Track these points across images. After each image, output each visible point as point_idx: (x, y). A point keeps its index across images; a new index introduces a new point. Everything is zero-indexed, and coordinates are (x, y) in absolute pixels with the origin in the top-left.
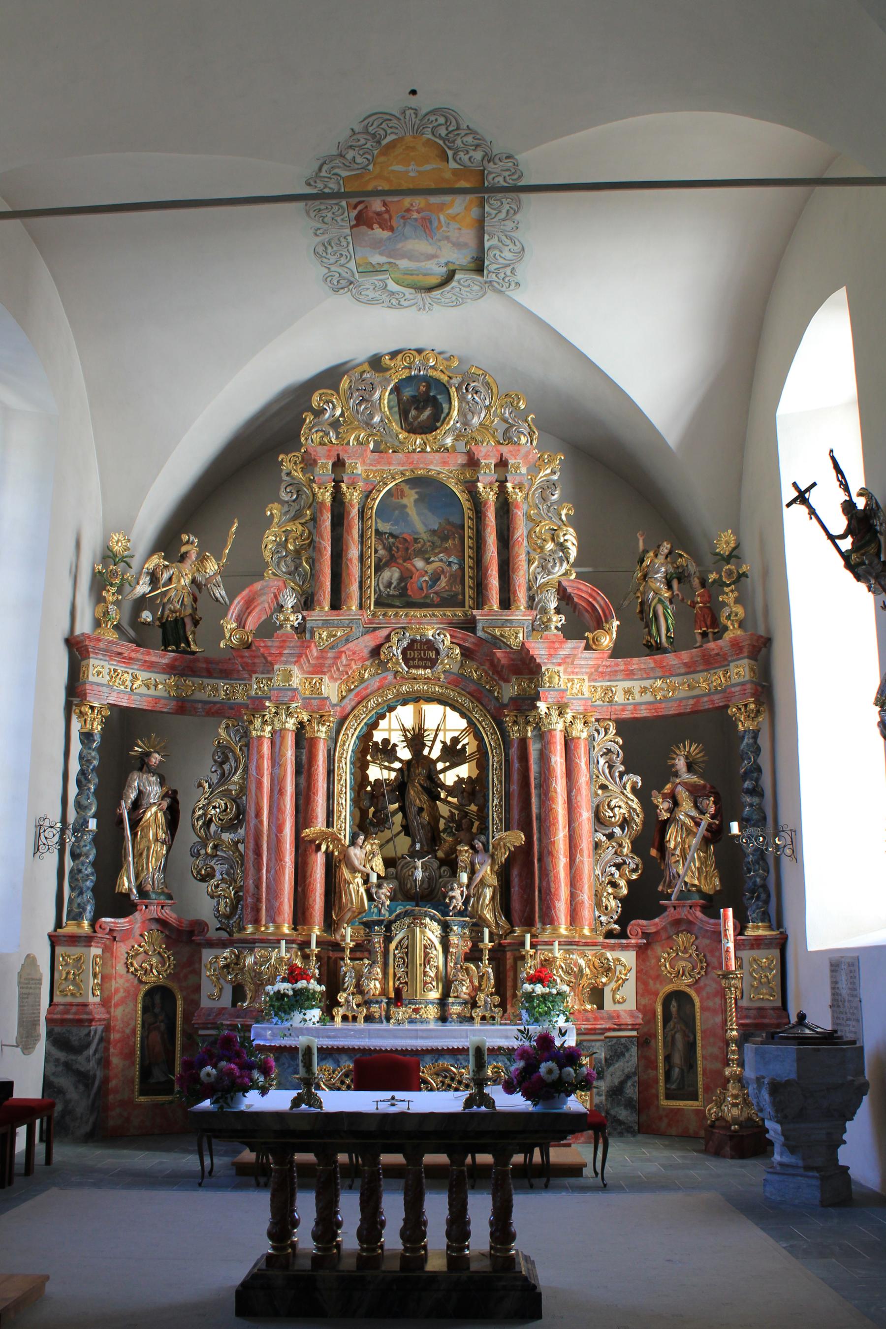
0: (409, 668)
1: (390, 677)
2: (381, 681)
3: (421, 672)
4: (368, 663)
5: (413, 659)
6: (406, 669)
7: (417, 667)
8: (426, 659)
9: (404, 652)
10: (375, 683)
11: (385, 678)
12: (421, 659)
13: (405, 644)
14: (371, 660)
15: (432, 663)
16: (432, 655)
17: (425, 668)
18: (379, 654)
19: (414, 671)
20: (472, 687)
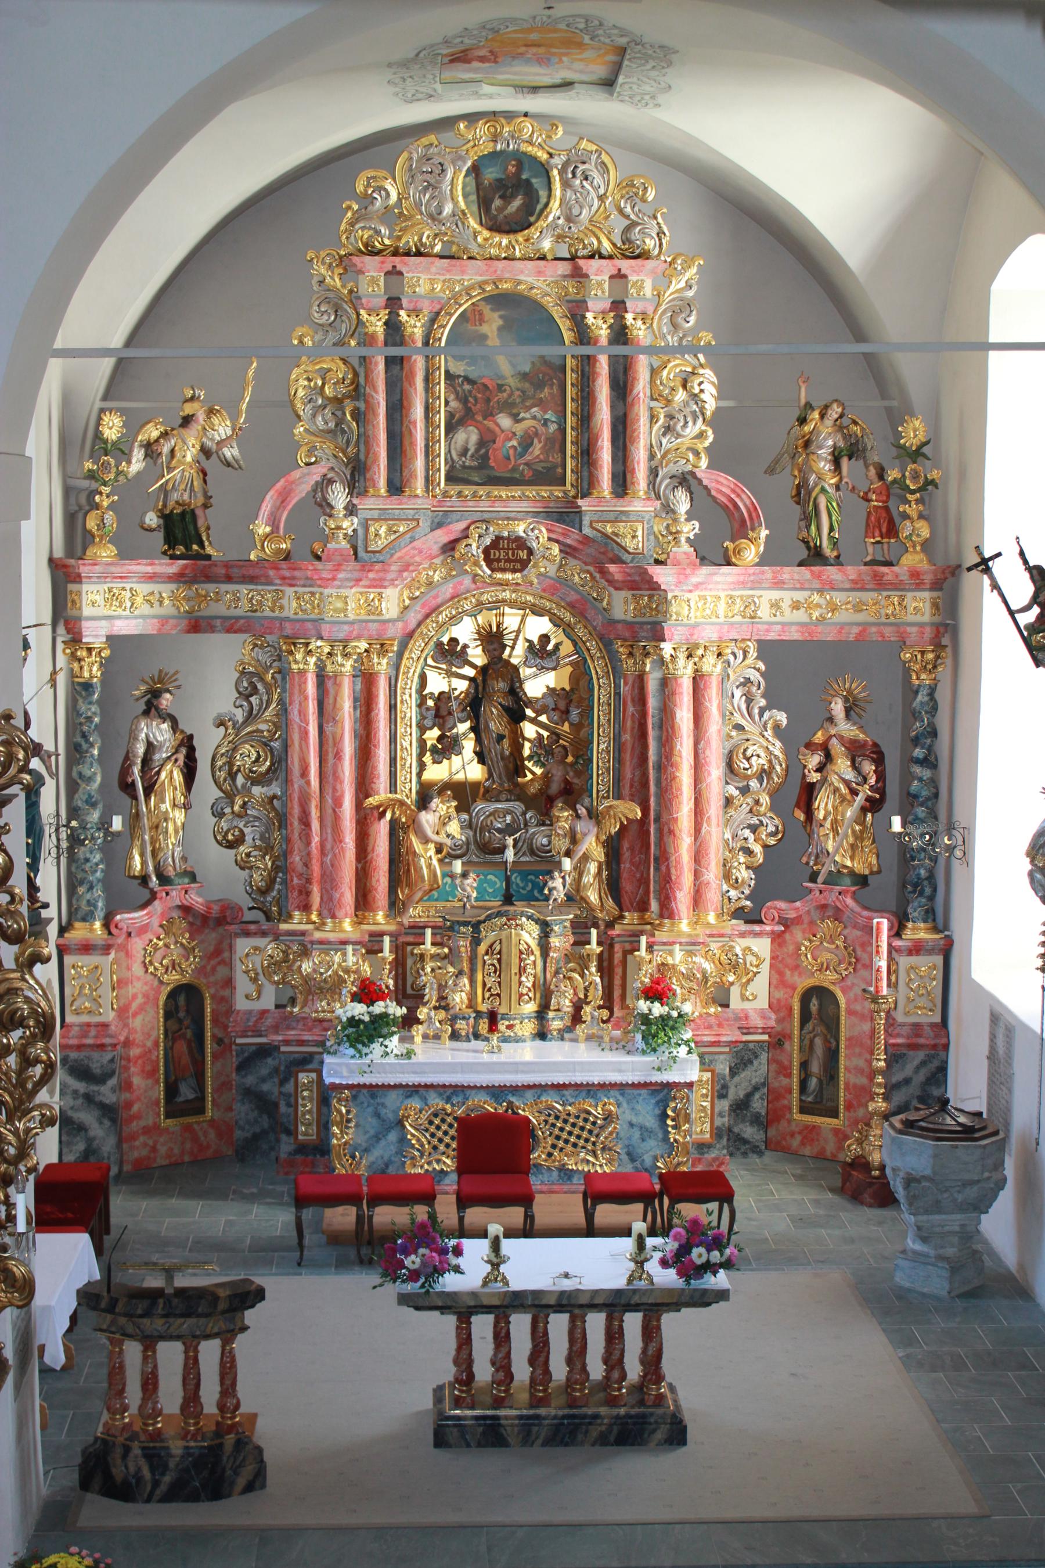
0: (493, 570)
1: (467, 581)
2: (454, 588)
3: (509, 576)
4: (437, 561)
5: (499, 560)
6: (489, 572)
7: (503, 570)
8: (515, 561)
9: (486, 551)
10: (447, 590)
11: (461, 583)
12: (508, 561)
13: (488, 541)
14: (441, 558)
15: (522, 565)
16: (523, 555)
17: (514, 571)
18: (453, 549)
19: (499, 575)
20: (573, 597)
